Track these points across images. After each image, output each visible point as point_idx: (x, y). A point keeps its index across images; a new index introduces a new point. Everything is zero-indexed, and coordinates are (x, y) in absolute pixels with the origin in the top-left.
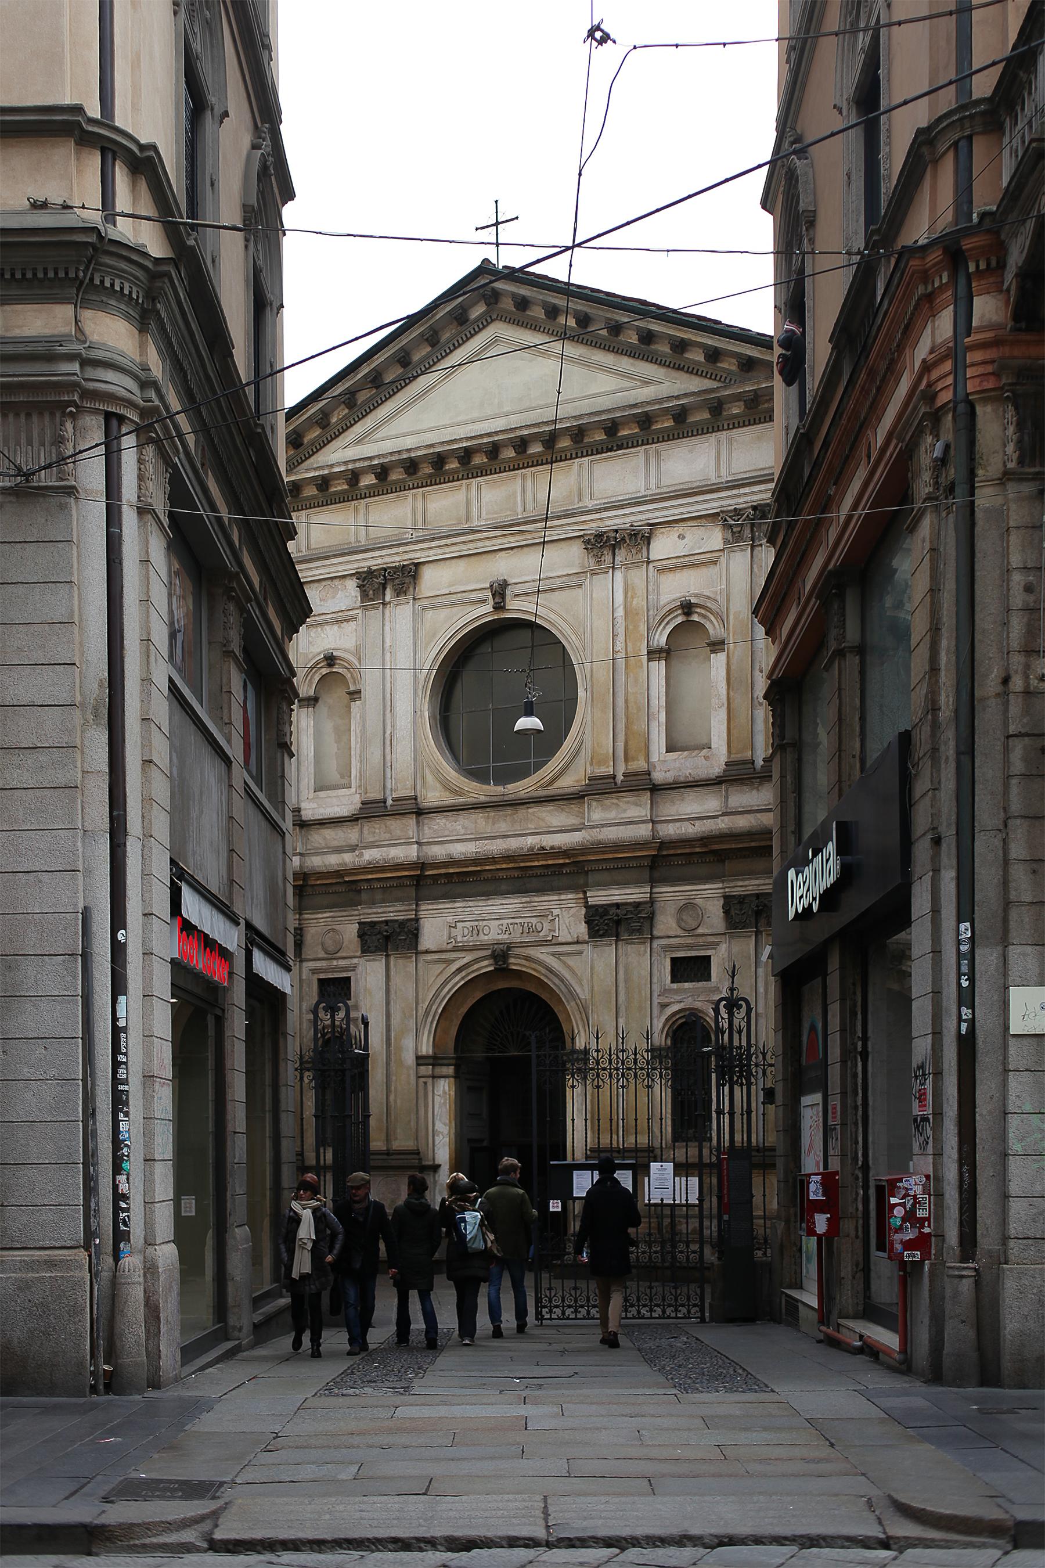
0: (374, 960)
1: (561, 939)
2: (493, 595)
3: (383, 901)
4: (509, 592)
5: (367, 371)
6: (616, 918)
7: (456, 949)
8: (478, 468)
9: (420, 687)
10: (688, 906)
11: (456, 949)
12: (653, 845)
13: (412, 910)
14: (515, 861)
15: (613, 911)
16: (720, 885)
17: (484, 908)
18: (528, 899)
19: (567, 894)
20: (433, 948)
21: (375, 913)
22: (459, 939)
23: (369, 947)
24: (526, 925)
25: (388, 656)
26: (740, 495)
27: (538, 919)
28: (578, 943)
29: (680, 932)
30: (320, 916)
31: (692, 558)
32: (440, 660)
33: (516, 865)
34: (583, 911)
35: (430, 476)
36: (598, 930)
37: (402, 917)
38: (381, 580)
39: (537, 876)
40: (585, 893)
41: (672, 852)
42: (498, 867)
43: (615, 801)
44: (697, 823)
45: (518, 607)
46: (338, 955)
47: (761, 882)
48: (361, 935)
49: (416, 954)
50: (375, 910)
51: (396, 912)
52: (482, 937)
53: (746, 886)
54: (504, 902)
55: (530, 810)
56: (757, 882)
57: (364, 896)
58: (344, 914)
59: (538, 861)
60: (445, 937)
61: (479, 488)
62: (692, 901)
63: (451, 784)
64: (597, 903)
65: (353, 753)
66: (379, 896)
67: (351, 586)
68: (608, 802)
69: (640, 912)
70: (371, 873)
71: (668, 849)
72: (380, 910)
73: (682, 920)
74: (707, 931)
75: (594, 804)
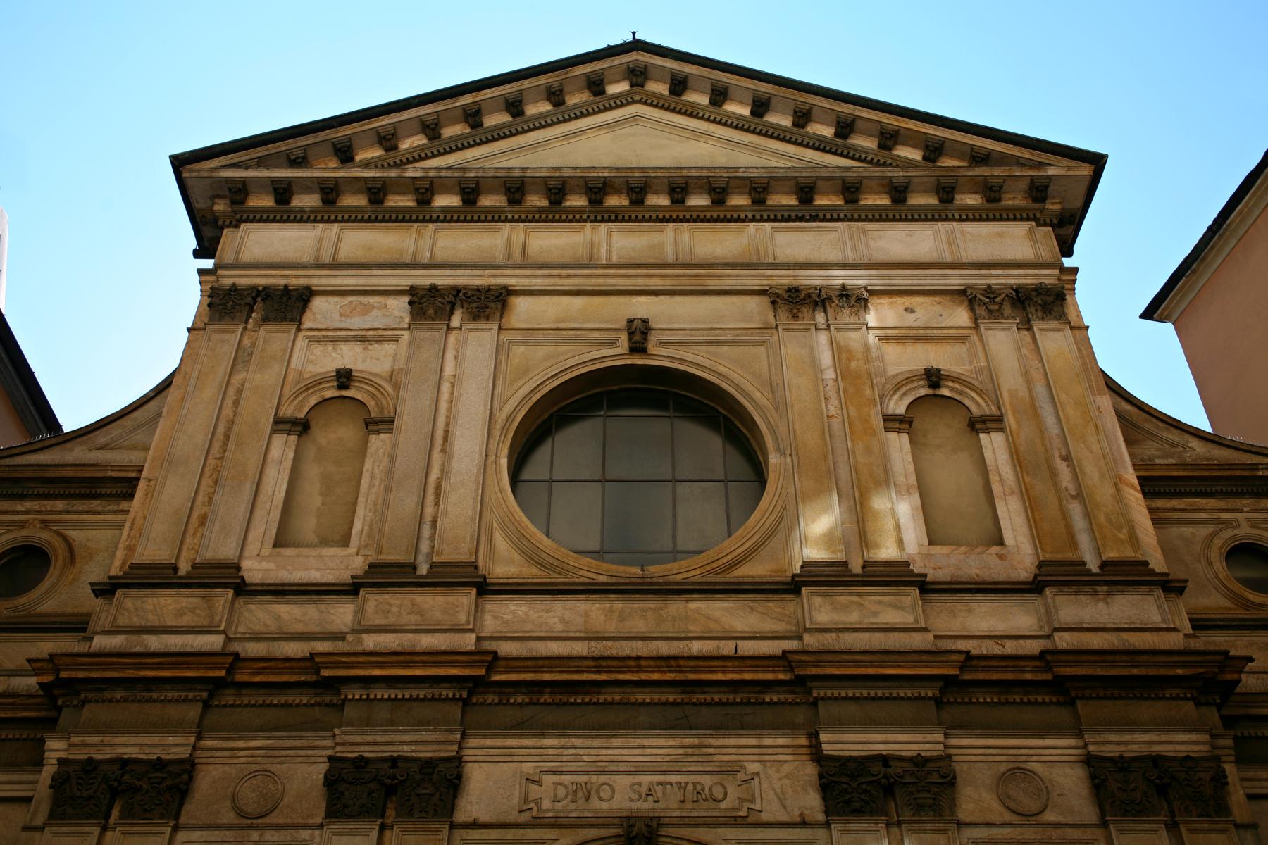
0: (351, 833)
1: (765, 817)
2: (631, 334)
3: (392, 723)
4: (653, 339)
5: (470, 101)
6: (884, 781)
7: (536, 823)
8: (613, 212)
9: (498, 426)
10: (1017, 773)
11: (536, 823)
12: (954, 657)
13: (451, 743)
14: (679, 669)
15: (876, 768)
16: (1072, 742)
17: (604, 752)
18: (696, 741)
19: (776, 735)
20: (484, 818)
21: (368, 744)
22: (546, 804)
23: (345, 806)
24: (690, 787)
25: (446, 387)
26: (992, 276)
27: (716, 778)
28: (804, 824)
29: (1008, 817)
30: (241, 744)
31: (929, 331)
32: (535, 399)
33: (680, 677)
34: (811, 770)
35: (541, 210)
36: (849, 802)
37: (429, 755)
38: (451, 298)
39: (709, 704)
40: (814, 735)
41: (981, 676)
42: (643, 676)
43: (855, 599)
44: (1008, 643)
45: (659, 356)
46: (267, 820)
47: (1154, 738)
48: (331, 782)
49: (453, 826)
50: (370, 738)
51: (416, 743)
52: (595, 803)
53: (1126, 743)
54: (646, 742)
55: (692, 606)
56: (1146, 738)
57: (349, 711)
58: (298, 743)
59: (724, 672)
60: (515, 800)
61: (609, 233)
62: (1022, 765)
63: (544, 555)
64: (841, 753)
65: (361, 499)
66: (382, 713)
67: (399, 306)
68: (843, 599)
69: (929, 773)
70: (381, 665)
71: (975, 669)
72: (380, 739)
73: (1009, 797)
74: (1062, 819)
75: (817, 600)
